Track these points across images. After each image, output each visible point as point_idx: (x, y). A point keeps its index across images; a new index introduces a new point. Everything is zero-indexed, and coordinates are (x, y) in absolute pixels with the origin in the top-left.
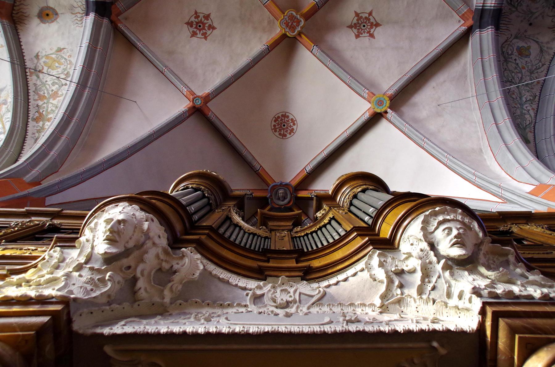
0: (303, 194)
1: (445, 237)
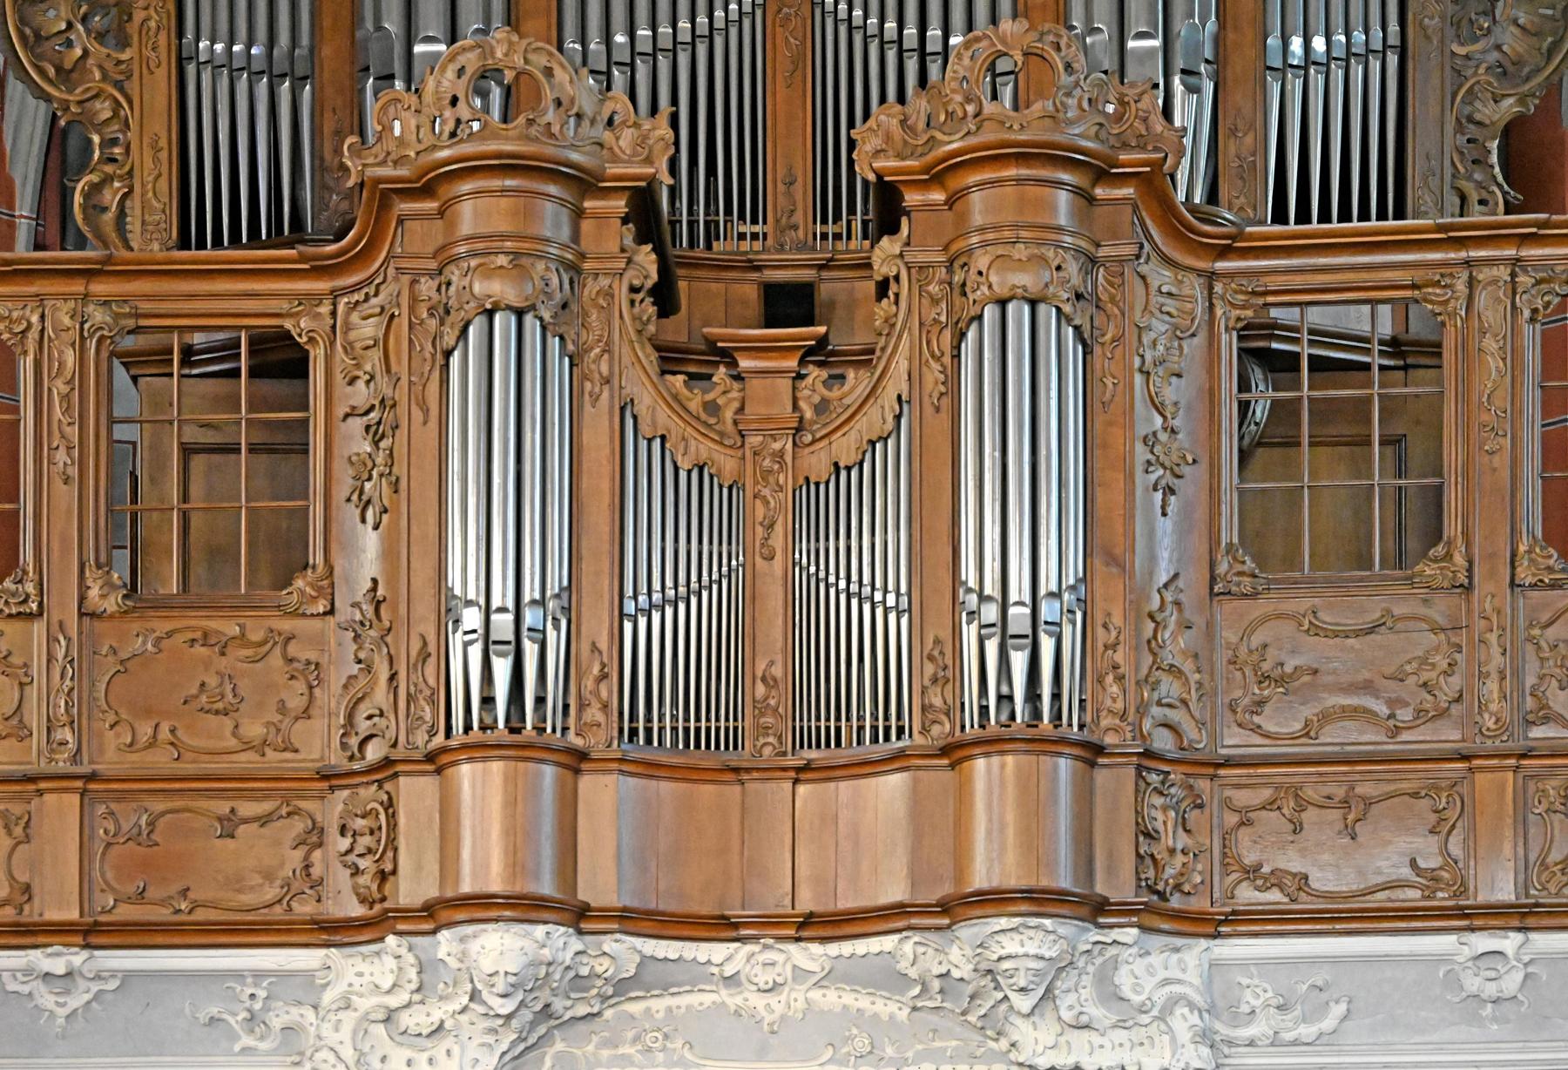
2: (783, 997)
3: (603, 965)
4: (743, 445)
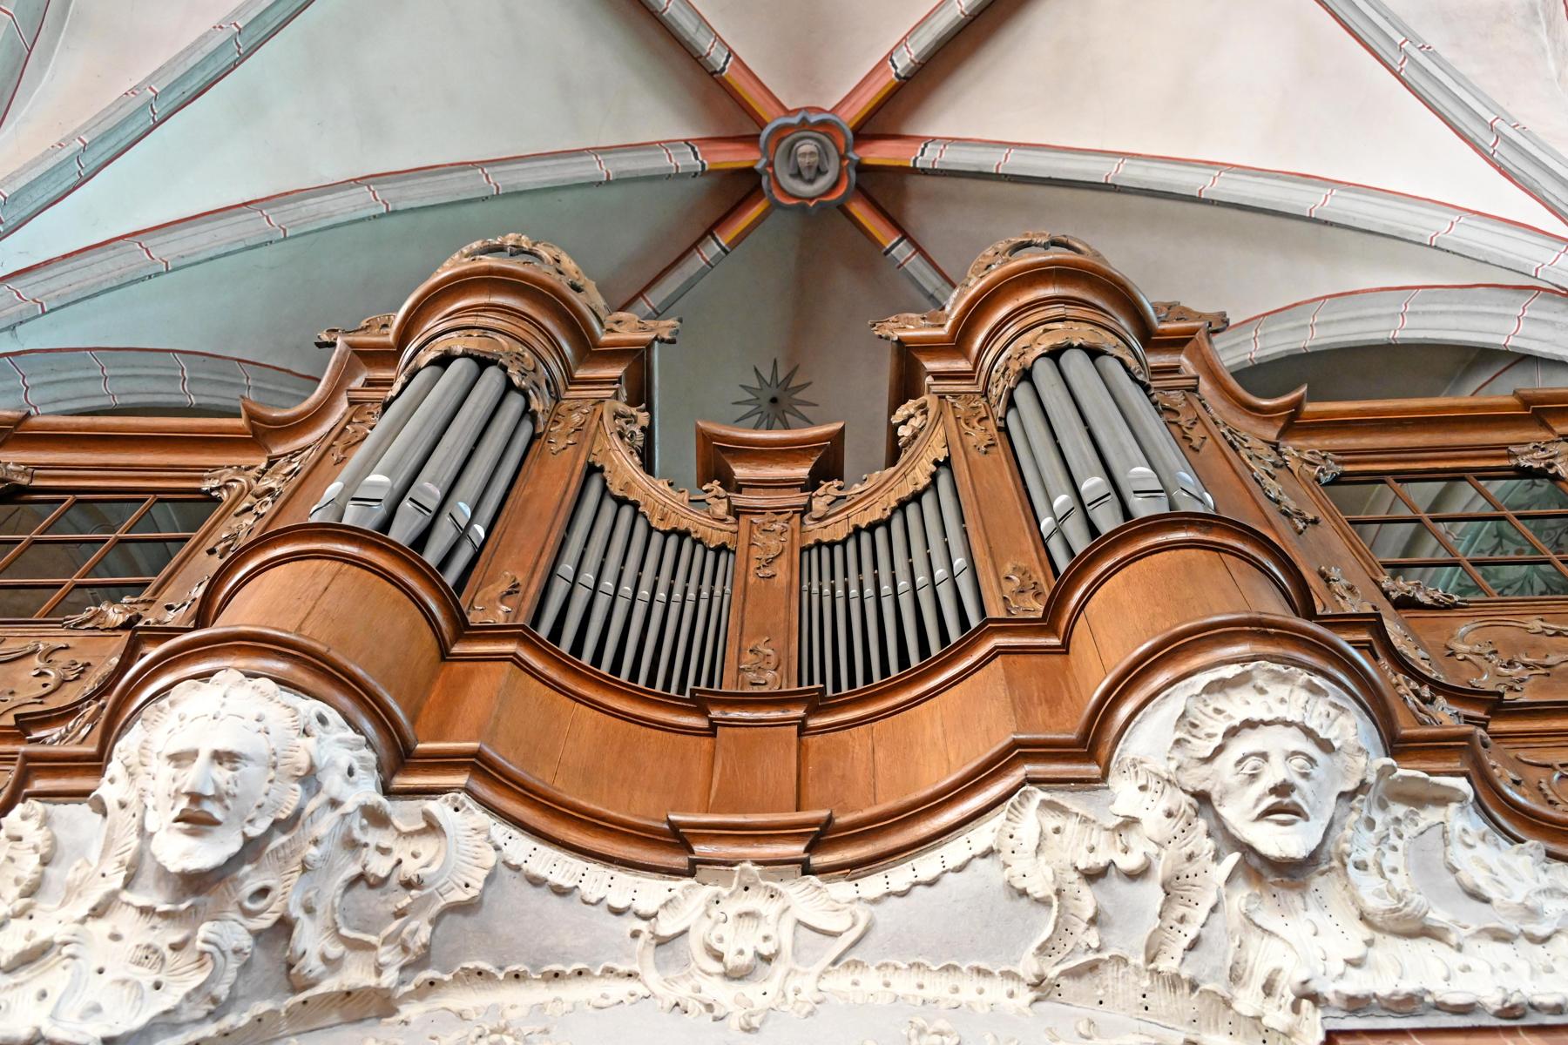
0: (880, 154)
1: (1242, 784)
2: (772, 987)
3: (418, 858)
4: (737, 523)
